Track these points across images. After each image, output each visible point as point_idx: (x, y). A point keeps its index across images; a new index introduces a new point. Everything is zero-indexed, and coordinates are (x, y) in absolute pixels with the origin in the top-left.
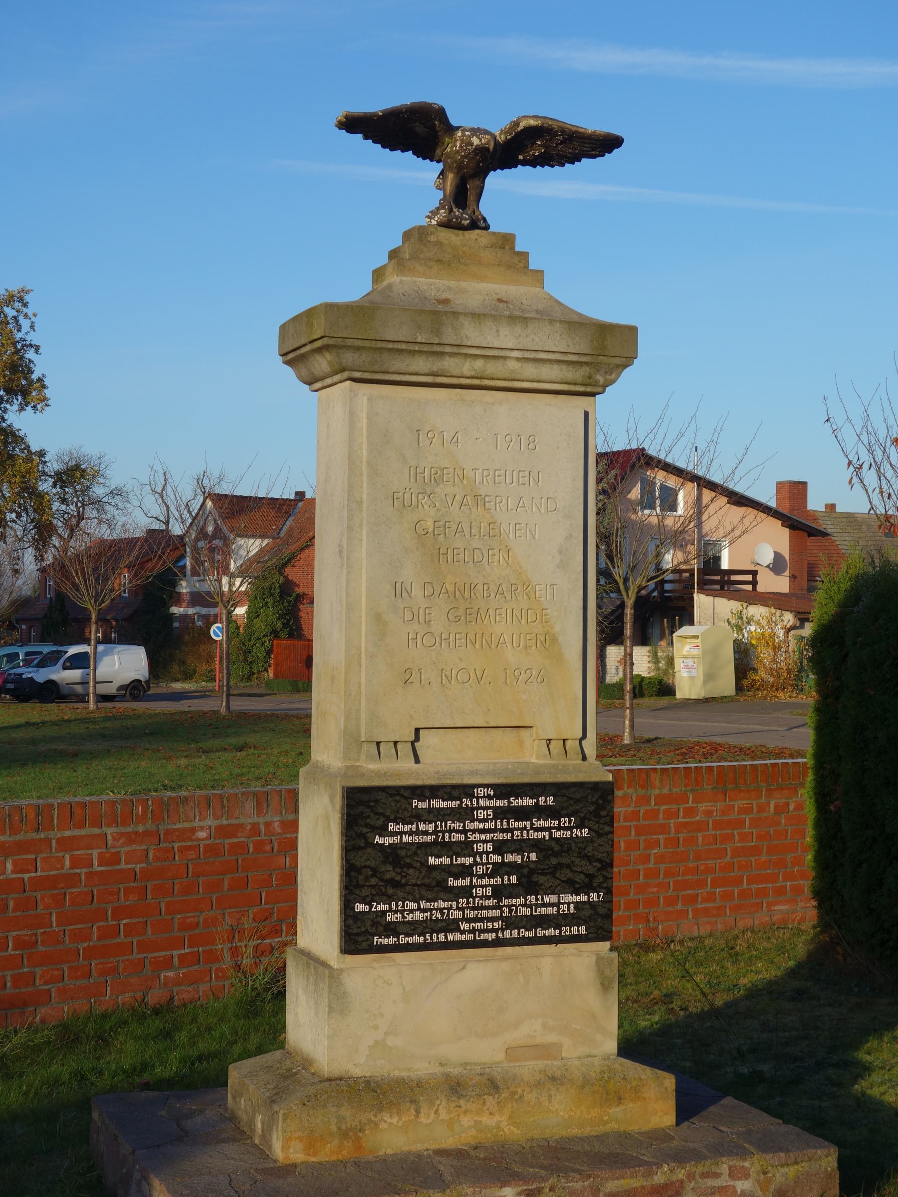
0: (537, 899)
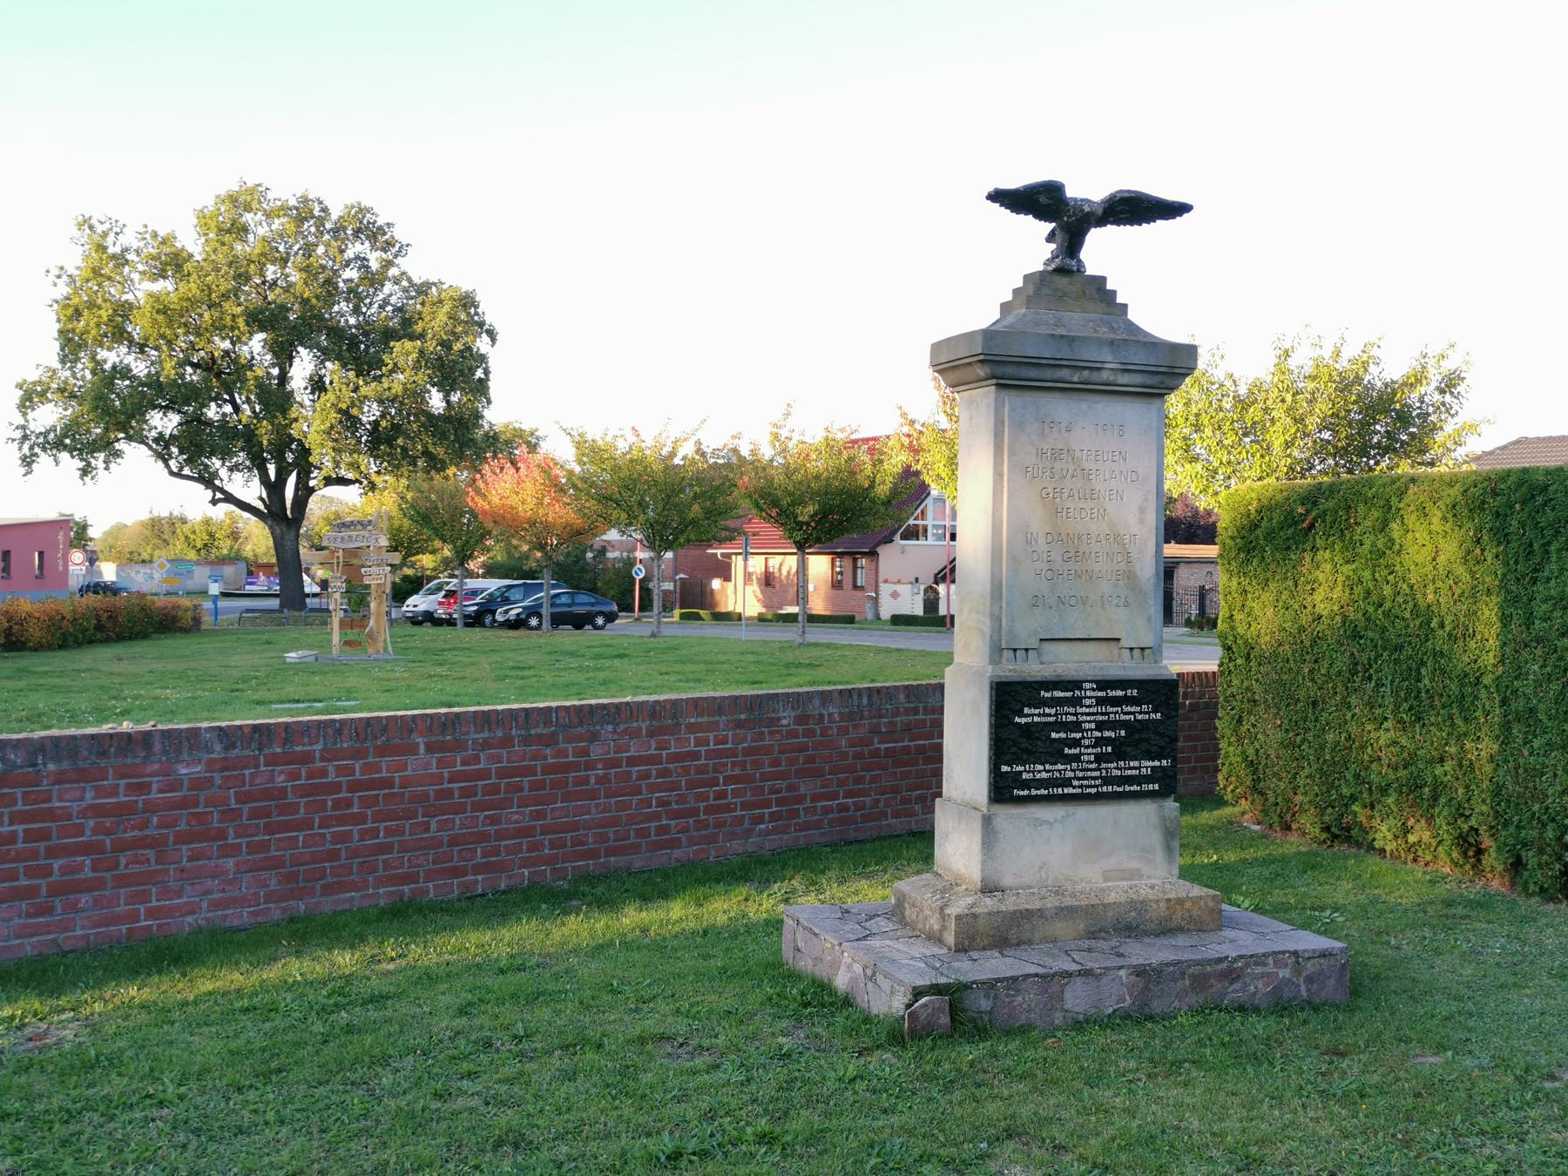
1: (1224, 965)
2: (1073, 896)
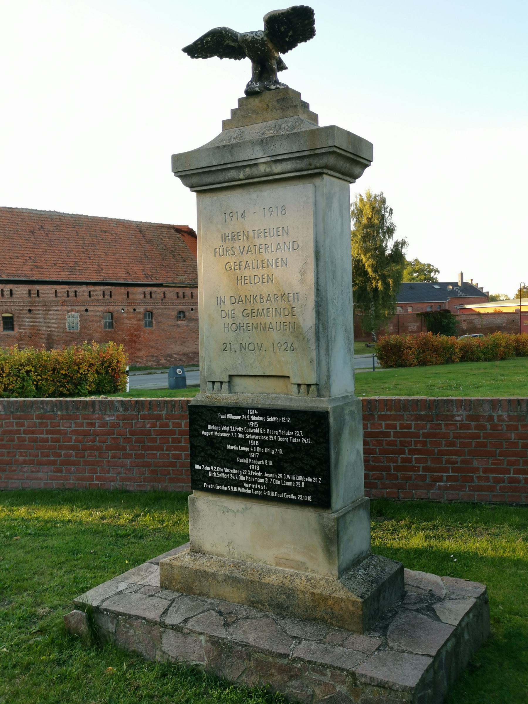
0: (283, 476)
1: (285, 661)
2: (245, 571)
